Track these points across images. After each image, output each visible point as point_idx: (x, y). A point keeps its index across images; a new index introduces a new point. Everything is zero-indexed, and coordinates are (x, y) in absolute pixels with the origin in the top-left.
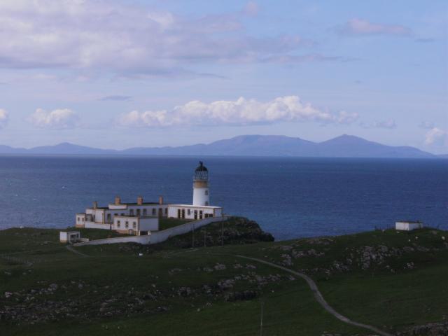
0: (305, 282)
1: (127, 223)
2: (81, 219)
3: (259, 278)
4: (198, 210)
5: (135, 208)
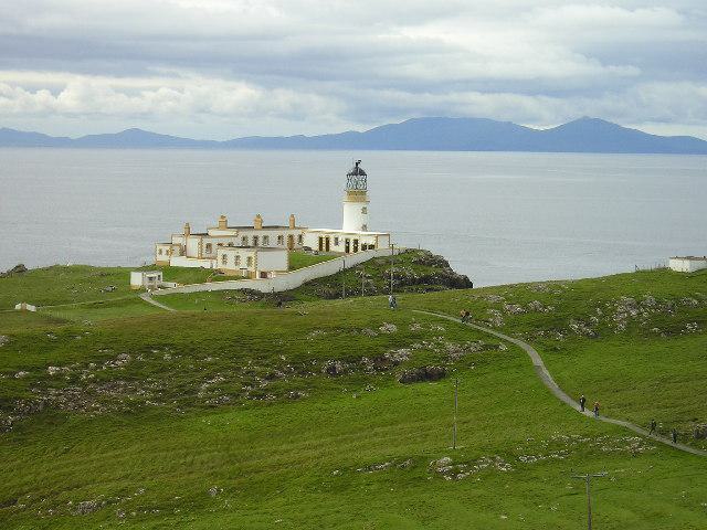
0: (523, 353)
2: (164, 252)
3: (450, 346)
4: (352, 239)
5: (250, 235)
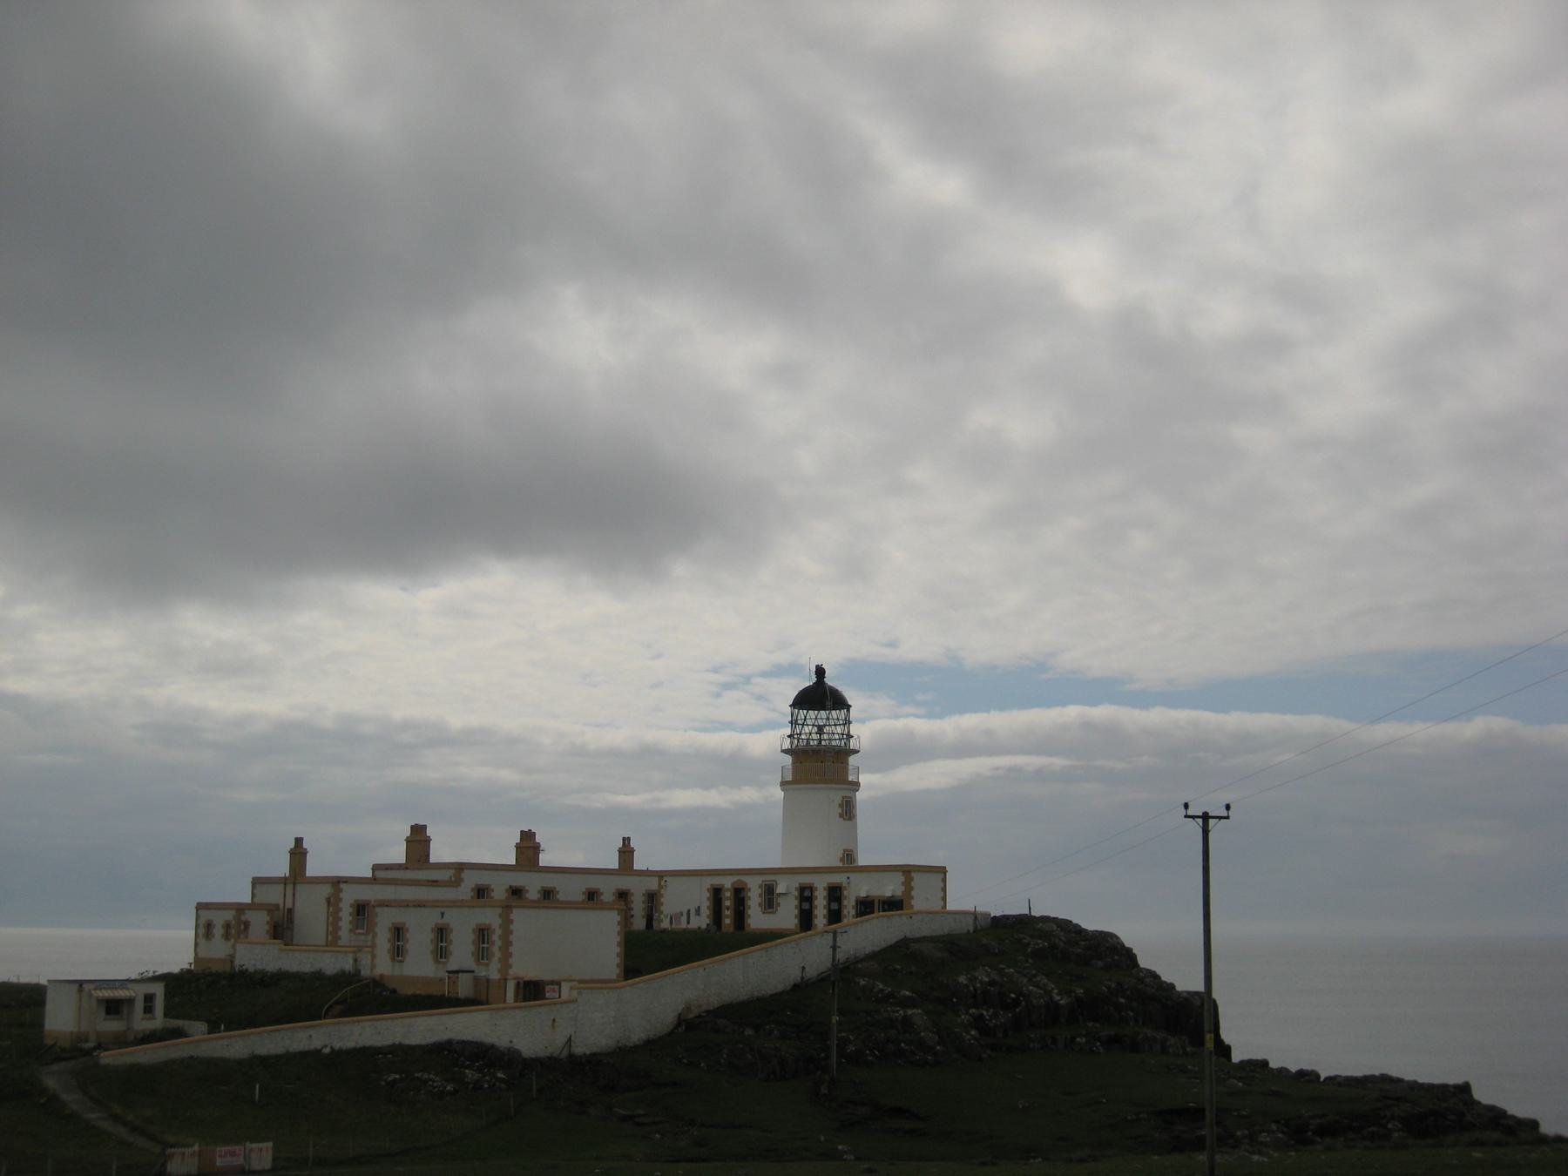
1: (441, 933)
2: (218, 931)
4: (821, 884)
